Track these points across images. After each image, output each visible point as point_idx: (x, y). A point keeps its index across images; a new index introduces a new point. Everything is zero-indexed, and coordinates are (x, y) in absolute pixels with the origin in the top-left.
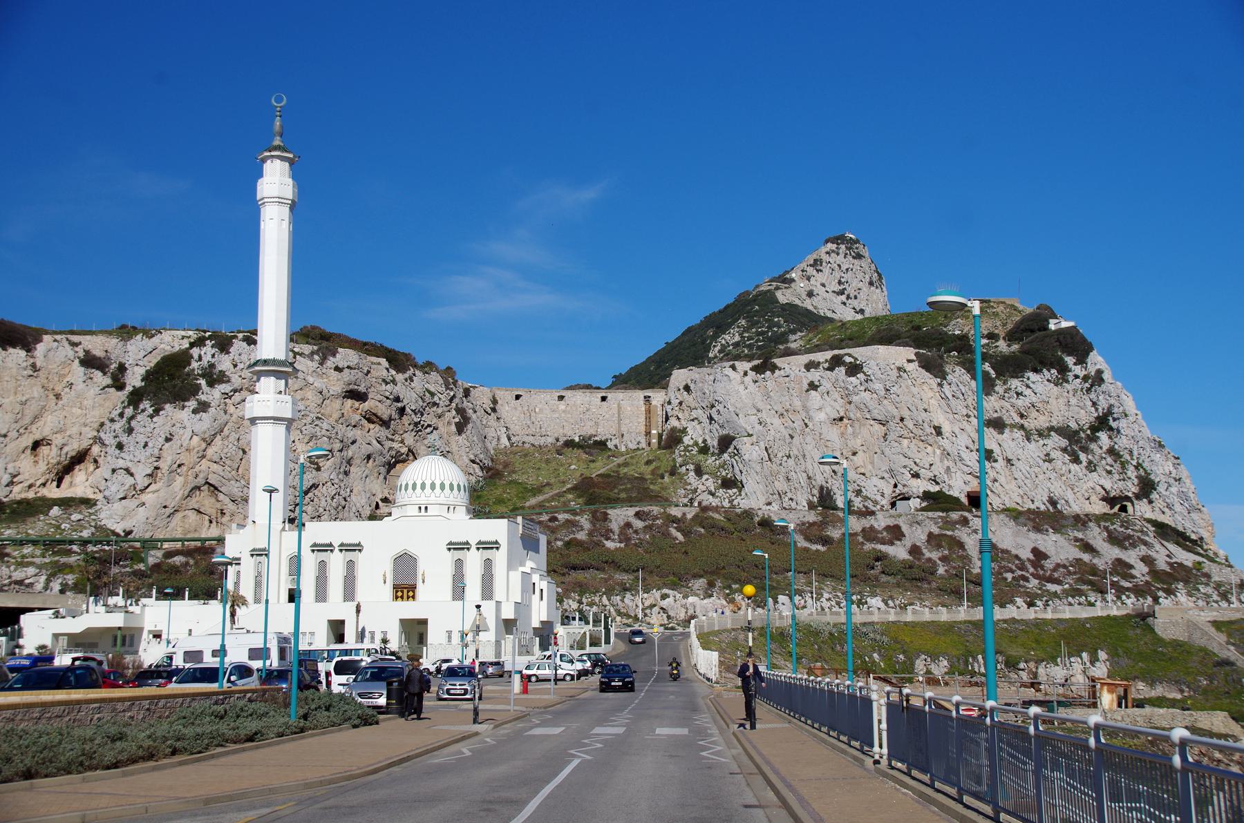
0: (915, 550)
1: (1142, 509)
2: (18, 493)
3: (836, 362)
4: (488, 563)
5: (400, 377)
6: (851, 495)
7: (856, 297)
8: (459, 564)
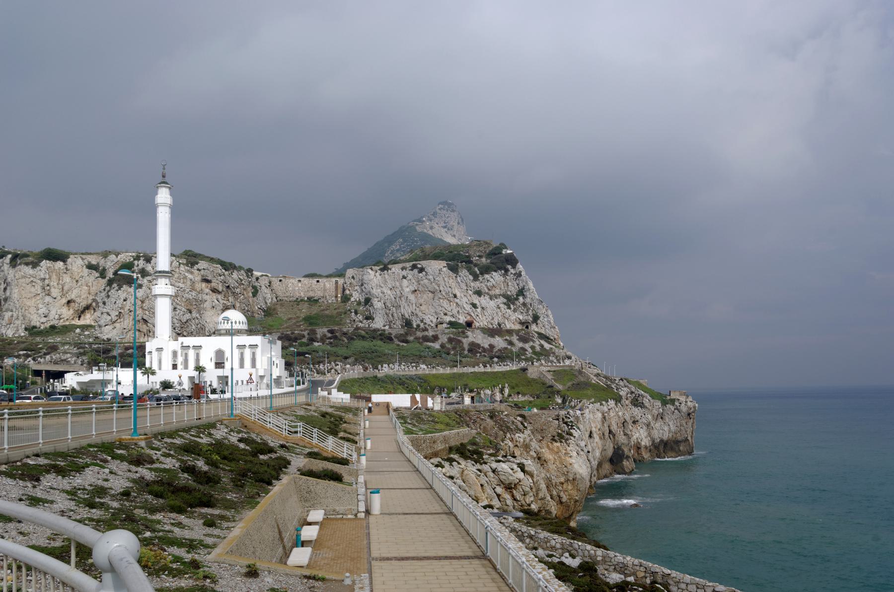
0: (442, 346)
1: (534, 327)
2: (61, 323)
3: (414, 267)
4: (254, 354)
5: (226, 273)
6: (419, 322)
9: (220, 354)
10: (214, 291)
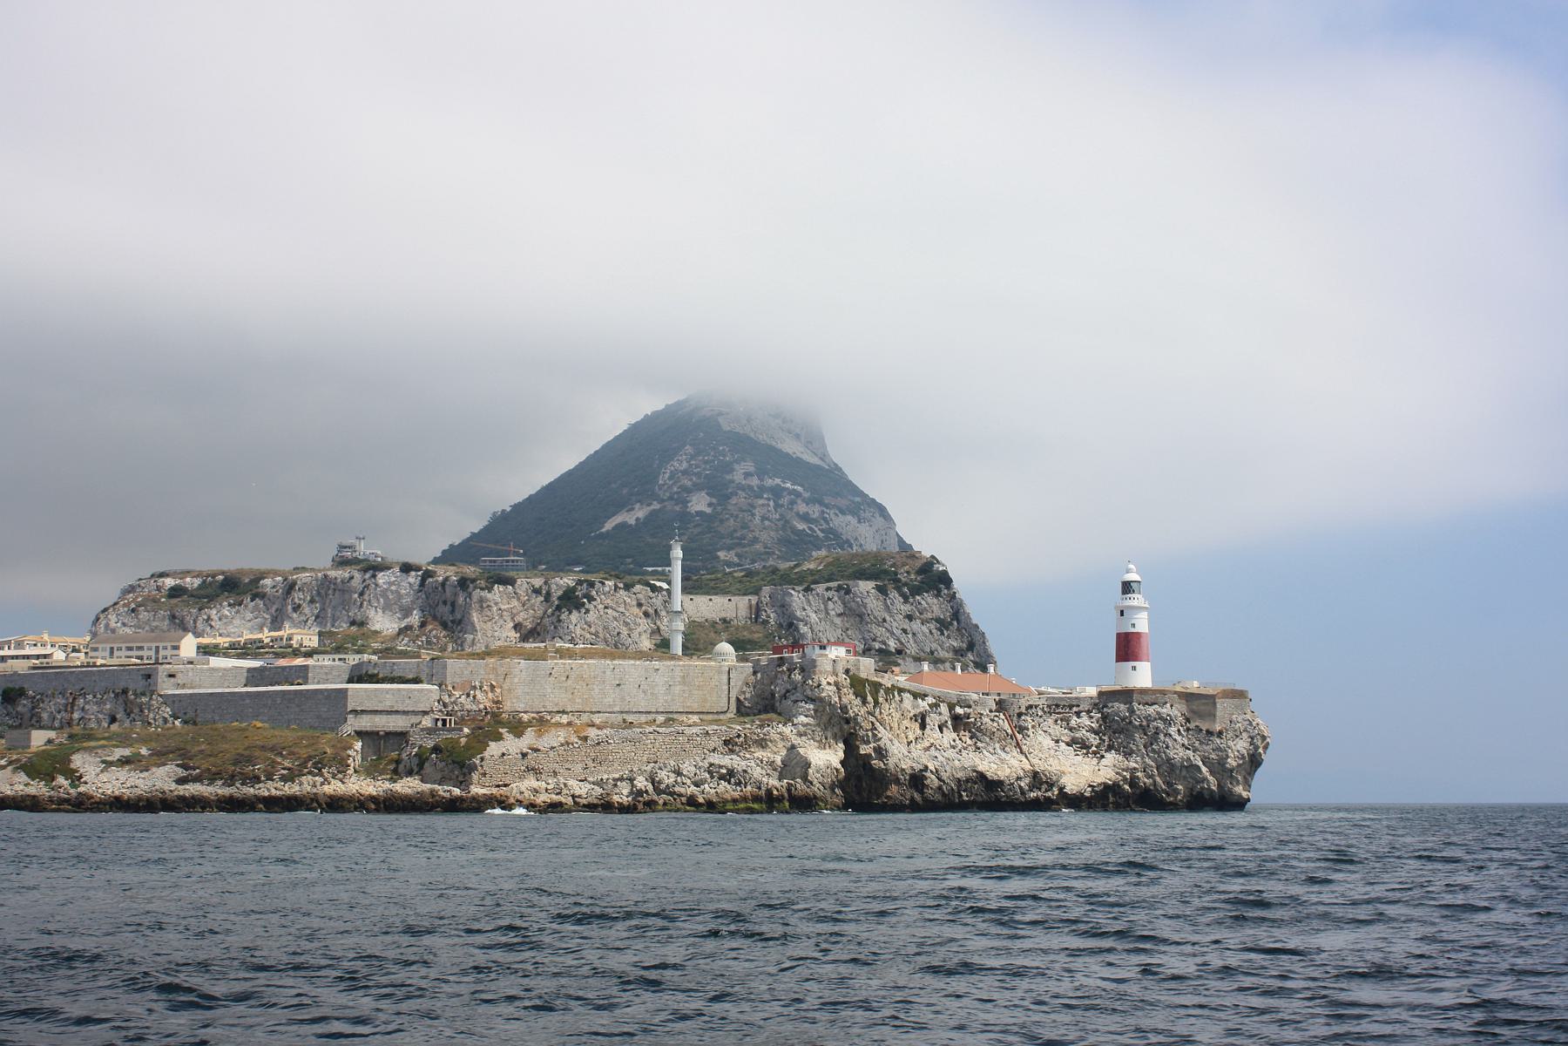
10: (646, 614)
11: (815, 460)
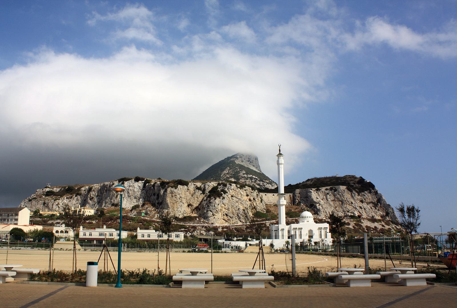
7: (252, 162)
8: (321, 232)
9: (311, 231)
10: (250, 200)
11: (259, 172)
